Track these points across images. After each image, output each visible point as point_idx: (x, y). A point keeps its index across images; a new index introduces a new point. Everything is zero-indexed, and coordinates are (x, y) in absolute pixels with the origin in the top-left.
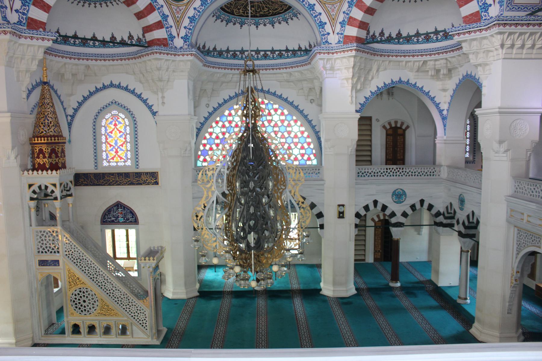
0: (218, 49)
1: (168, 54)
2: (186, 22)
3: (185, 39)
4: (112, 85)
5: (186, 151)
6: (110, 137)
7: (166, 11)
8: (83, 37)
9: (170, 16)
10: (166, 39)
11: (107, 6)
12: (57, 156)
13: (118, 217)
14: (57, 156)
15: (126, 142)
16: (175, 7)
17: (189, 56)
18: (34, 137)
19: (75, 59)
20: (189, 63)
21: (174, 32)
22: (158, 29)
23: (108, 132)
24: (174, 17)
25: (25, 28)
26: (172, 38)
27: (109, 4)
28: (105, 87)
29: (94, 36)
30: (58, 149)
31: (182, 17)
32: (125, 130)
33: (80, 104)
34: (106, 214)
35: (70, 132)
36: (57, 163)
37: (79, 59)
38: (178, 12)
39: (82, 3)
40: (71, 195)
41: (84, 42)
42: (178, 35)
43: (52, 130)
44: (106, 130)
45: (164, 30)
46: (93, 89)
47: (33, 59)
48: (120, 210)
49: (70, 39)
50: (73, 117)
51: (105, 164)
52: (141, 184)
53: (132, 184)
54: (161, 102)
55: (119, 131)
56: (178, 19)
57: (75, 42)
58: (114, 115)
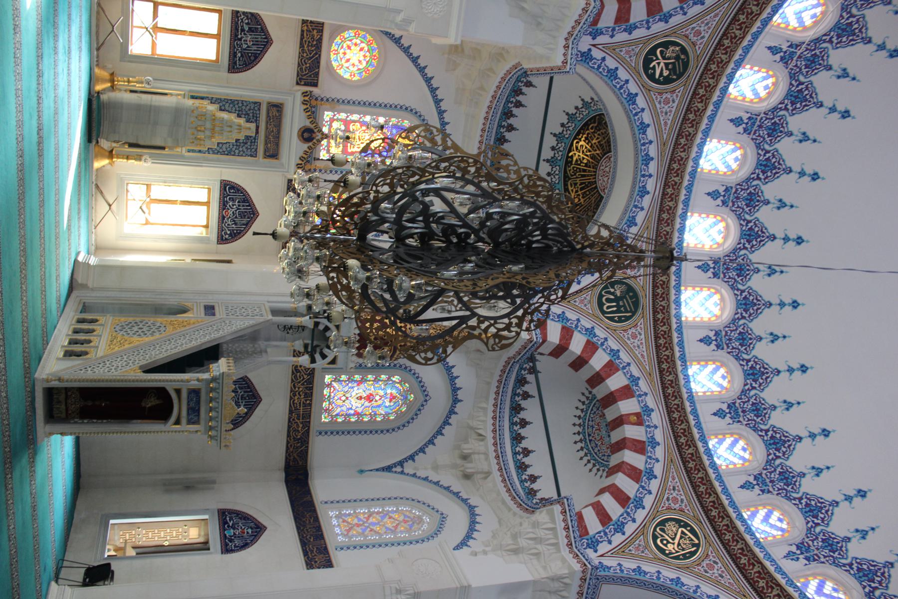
1: (567, 528)
2: (630, 564)
4: (471, 509)
6: (383, 517)
7: (630, 528)
9: (624, 537)
11: (591, 470)
13: (234, 529)
16: (642, 543)
17: (579, 565)
20: (566, 572)
21: (603, 548)
22: (597, 514)
26: (593, 544)
27: (595, 470)
28: (465, 501)
31: (633, 557)
32: (401, 532)
34: (238, 515)
35: (377, 470)
38: (637, 549)
44: (393, 512)
45: (600, 528)
48: (250, 531)
50: (402, 473)
52: (305, 553)
53: (304, 543)
54: (477, 550)
55: (397, 525)
58: (422, 519)
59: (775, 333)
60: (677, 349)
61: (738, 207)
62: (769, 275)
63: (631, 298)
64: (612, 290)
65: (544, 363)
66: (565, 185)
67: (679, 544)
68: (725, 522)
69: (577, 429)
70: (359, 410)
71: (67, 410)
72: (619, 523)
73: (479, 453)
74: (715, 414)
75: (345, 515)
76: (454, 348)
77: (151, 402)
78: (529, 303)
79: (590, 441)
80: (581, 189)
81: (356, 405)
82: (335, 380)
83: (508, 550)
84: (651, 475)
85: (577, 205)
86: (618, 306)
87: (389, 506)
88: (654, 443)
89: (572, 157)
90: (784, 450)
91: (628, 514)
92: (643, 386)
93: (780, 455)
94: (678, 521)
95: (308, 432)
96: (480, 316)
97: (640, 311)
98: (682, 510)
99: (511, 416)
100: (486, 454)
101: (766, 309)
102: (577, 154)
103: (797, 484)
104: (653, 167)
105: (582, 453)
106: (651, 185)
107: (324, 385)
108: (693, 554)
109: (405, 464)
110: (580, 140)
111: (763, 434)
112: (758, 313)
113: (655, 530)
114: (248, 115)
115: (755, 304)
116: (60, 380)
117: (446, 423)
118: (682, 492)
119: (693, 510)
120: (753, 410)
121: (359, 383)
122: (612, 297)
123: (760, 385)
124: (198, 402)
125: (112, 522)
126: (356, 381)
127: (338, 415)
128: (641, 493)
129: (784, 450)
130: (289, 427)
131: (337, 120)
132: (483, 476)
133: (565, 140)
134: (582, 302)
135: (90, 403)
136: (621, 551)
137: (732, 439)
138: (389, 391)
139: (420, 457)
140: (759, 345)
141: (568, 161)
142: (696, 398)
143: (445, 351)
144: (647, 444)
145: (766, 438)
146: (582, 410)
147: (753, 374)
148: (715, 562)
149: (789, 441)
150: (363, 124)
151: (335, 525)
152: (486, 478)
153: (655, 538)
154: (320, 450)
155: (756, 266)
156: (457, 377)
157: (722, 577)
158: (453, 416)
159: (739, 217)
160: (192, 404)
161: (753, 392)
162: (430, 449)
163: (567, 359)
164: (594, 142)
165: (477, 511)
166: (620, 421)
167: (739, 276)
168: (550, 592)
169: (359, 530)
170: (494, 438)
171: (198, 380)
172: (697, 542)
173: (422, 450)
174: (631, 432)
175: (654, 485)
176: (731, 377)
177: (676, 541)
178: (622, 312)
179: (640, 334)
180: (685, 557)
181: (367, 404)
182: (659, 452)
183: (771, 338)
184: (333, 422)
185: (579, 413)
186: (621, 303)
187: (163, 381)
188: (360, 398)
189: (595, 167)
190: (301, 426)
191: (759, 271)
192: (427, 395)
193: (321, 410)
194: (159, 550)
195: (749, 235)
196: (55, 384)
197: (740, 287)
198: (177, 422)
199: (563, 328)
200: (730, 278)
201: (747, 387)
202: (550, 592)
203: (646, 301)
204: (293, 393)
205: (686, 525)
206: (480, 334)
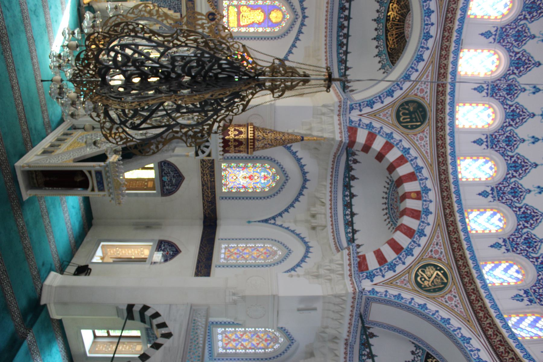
0: (371, 341)
1: (350, 265)
2: (393, 292)
3: (373, 291)
5: (234, 294)
6: (252, 250)
8: (354, 222)
9: (395, 274)
10: (367, 269)
11: (389, 228)
12: (235, 146)
14: (235, 135)
15: (246, 259)
16: (407, 279)
17: (352, 289)
18: (254, 127)
19: (331, 213)
20: (344, 292)
21: (378, 279)
23: (259, 249)
24: (395, 278)
25: (348, 125)
29: (356, 231)
30: (242, 148)
32: (260, 260)
33: (287, 228)
35: (259, 221)
36: (229, 146)
37: (331, 217)
38: (402, 282)
39: (385, 206)
40: (197, 155)
41: (349, 224)
42: (376, 284)
43: (260, 134)
45: (378, 266)
46: (302, 236)
47: (322, 130)
48: (171, 253)
49: (351, 228)
50: (274, 224)
51: (223, 246)
52: (197, 267)
53: (199, 262)
56: (394, 283)
57: (348, 215)
59: (536, 136)
60: (448, 147)
61: (508, 42)
62: (534, 93)
63: (421, 112)
64: (407, 107)
65: (361, 156)
66: (386, 36)
67: (433, 282)
68: (466, 270)
69: (385, 201)
70: (245, 185)
71: (37, 181)
72: (392, 264)
73: (321, 214)
74: (480, 194)
75: (232, 247)
76: (164, 145)
77: (79, 179)
78: (217, 115)
79: (391, 209)
80: (396, 38)
81: (243, 182)
82: (229, 167)
83: (314, 276)
84: (422, 234)
85: (393, 49)
86: (411, 118)
87: (259, 243)
88: (427, 212)
89: (389, 16)
90: (532, 222)
91: (400, 259)
92: (425, 173)
93: (528, 225)
94: (436, 267)
95: (214, 198)
96: (181, 124)
97: (427, 121)
98: (440, 259)
99: (344, 191)
100: (325, 214)
101: (530, 119)
102: (393, 13)
103: (538, 247)
104: (434, 18)
105: (386, 217)
106: (433, 31)
107: (221, 170)
108: (440, 289)
109: (277, 219)
110: (394, 3)
111: (517, 210)
112: (523, 121)
113: (418, 271)
114: (175, 8)
115: (521, 115)
116: (29, 166)
117: (300, 194)
118: (442, 247)
119: (448, 259)
120: (512, 193)
121: (243, 168)
122: (407, 112)
123: (520, 174)
124: (102, 179)
125: (102, 243)
126: (241, 167)
127: (232, 188)
128: (412, 245)
129: (532, 222)
130: (203, 194)
131: (232, 5)
132: (322, 228)
133: (385, 5)
134: (385, 115)
135: (48, 179)
136: (390, 283)
137: (492, 212)
138: (263, 174)
139: (285, 215)
140: (521, 146)
141: (388, 19)
142: (460, 183)
143: (157, 147)
144: (422, 213)
145: (518, 213)
146: (388, 188)
147: (515, 167)
148: (455, 296)
149: (537, 216)
150: (248, 6)
151: (222, 252)
152: (323, 230)
153: (417, 276)
154: (222, 207)
155: (523, 86)
156: (305, 165)
157: (456, 306)
158: (305, 190)
159: (509, 50)
160: (99, 180)
161: (513, 180)
162: (291, 210)
163: (372, 155)
164: (402, 3)
165: (311, 250)
166: (405, 196)
167: (508, 94)
168: (334, 304)
169: (235, 256)
170: (331, 204)
171: (100, 166)
172: (445, 281)
173: (286, 210)
174: (411, 204)
175: (423, 241)
176: (498, 168)
177: (432, 279)
178: (413, 122)
179: (426, 137)
180: (435, 291)
181: (250, 181)
182: (431, 219)
183: (532, 140)
184: (230, 192)
185: (386, 190)
186: (413, 116)
187: (81, 166)
188: (245, 178)
189: (404, 22)
190: (210, 194)
191: (525, 90)
192: (287, 177)
193: (222, 185)
194: (129, 260)
195: (518, 63)
196: (27, 168)
197: (509, 103)
198: (93, 190)
199: (369, 133)
200: (500, 96)
201: (508, 176)
202: (334, 304)
203: (431, 114)
204: (203, 174)
205: (441, 269)
206: (182, 136)
